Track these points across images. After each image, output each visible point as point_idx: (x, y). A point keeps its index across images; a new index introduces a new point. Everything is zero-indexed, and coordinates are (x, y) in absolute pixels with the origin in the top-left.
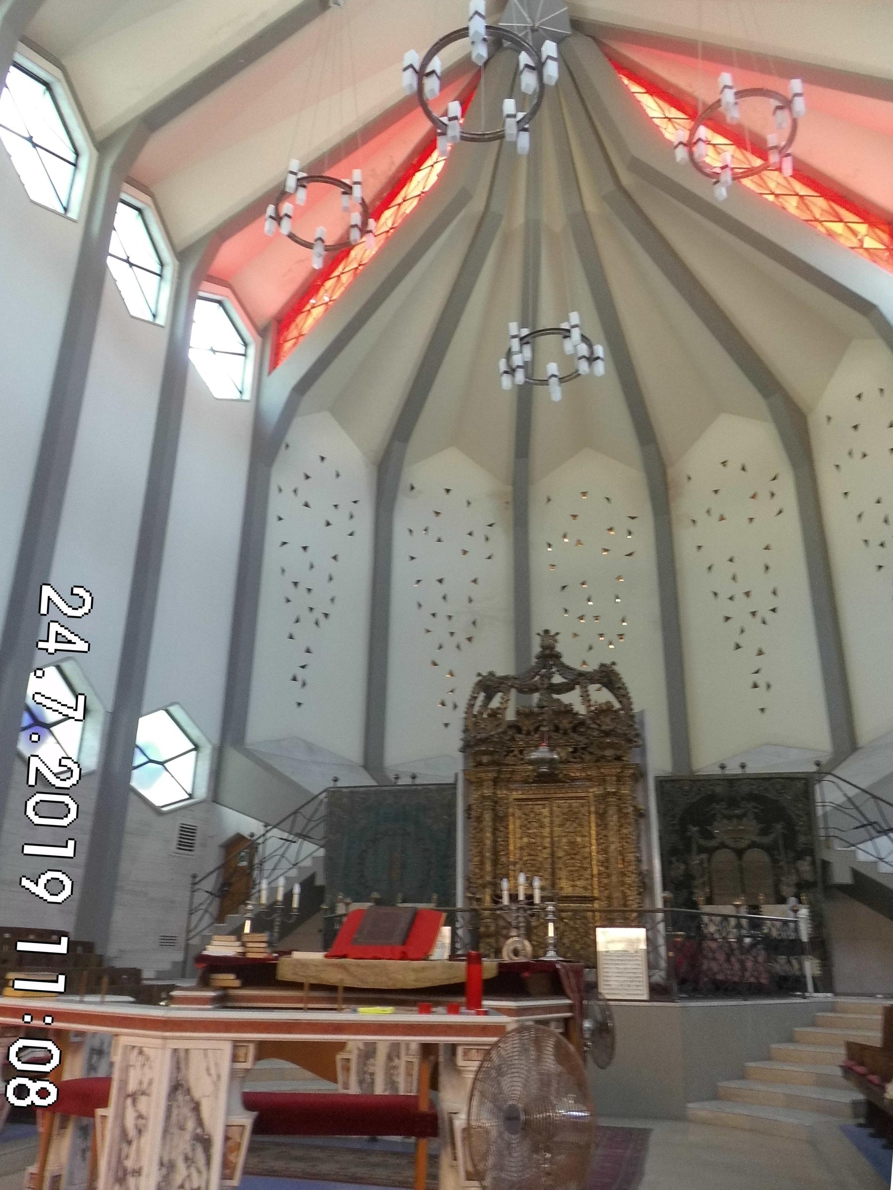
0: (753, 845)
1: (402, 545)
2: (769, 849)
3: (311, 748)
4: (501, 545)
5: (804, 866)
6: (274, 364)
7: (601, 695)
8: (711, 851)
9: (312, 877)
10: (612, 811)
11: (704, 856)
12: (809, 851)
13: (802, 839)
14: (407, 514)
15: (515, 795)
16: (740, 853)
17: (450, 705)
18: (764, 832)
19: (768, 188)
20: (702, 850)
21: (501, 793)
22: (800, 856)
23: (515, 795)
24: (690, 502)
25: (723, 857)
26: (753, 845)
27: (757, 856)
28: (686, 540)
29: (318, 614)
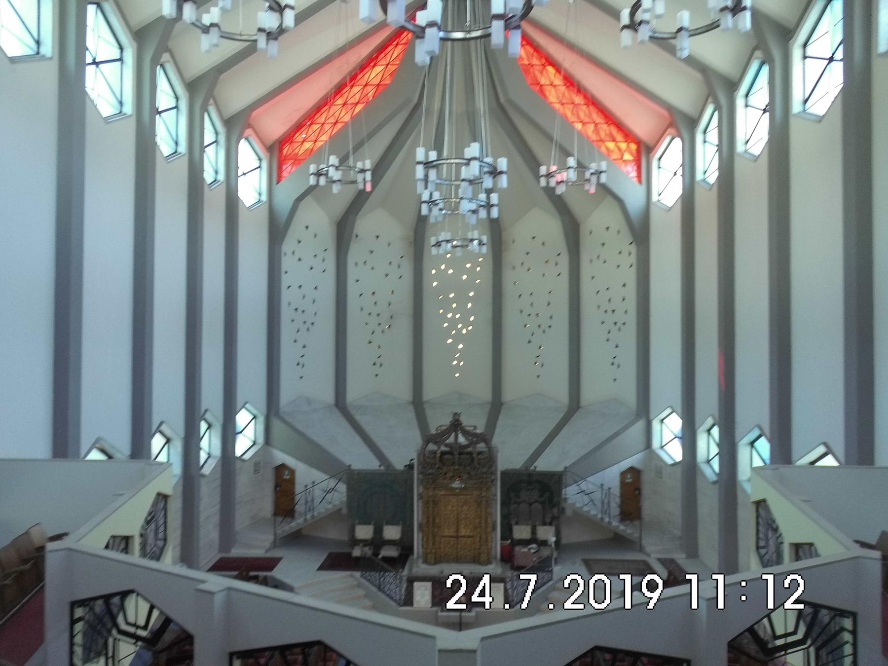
0: (536, 501)
1: (352, 273)
2: (543, 503)
3: (309, 401)
4: (407, 270)
5: (555, 510)
6: (278, 182)
7: (481, 446)
8: (519, 504)
9: (340, 510)
10: (484, 503)
11: (516, 505)
12: (558, 504)
13: (555, 499)
14: (354, 254)
15: (442, 493)
16: (530, 504)
17: (378, 365)
18: (541, 496)
19: (579, 117)
20: (515, 503)
21: (437, 492)
22: (553, 507)
23: (442, 493)
24: (513, 255)
25: (524, 507)
26: (536, 501)
27: (537, 506)
28: (509, 277)
29: (308, 324)
